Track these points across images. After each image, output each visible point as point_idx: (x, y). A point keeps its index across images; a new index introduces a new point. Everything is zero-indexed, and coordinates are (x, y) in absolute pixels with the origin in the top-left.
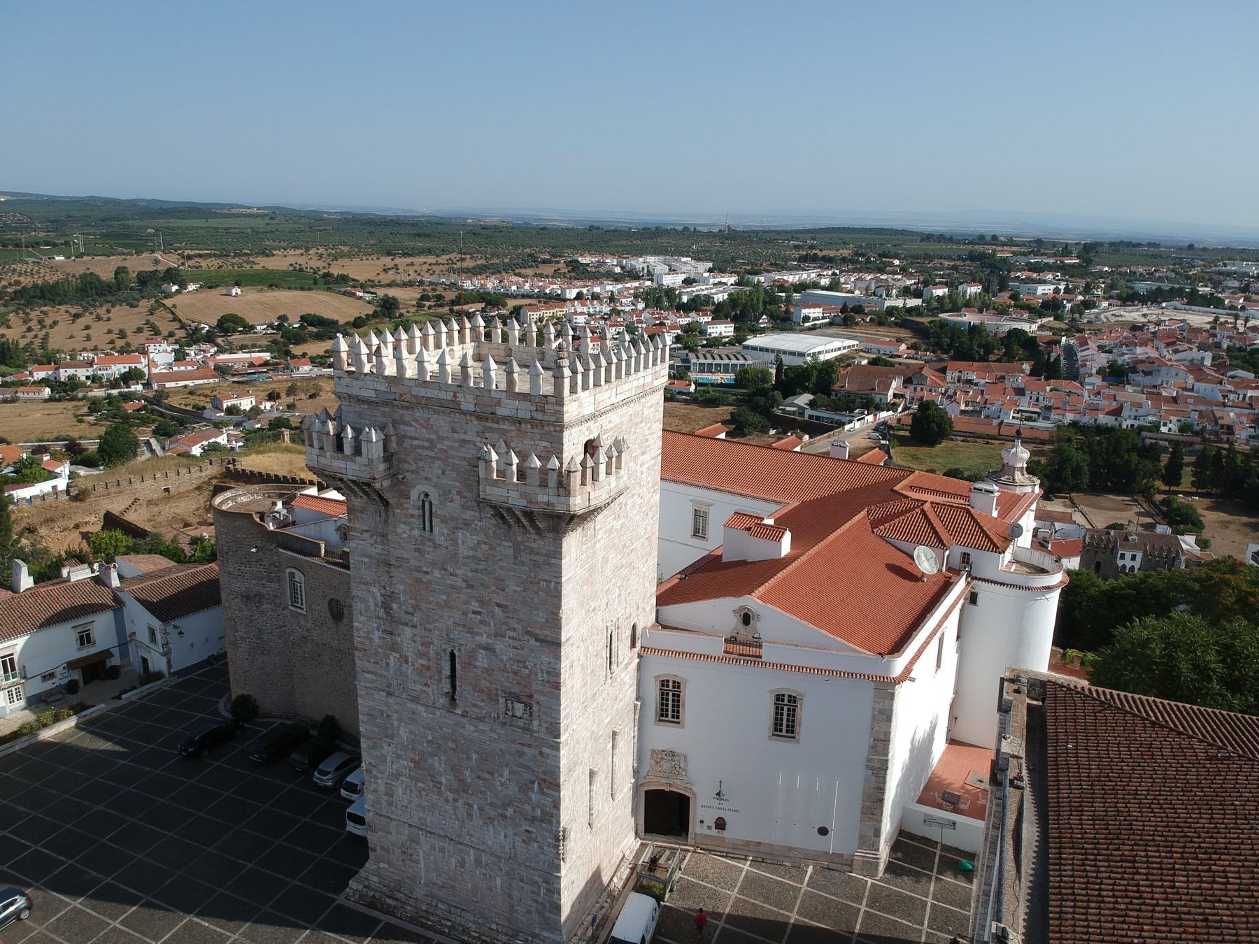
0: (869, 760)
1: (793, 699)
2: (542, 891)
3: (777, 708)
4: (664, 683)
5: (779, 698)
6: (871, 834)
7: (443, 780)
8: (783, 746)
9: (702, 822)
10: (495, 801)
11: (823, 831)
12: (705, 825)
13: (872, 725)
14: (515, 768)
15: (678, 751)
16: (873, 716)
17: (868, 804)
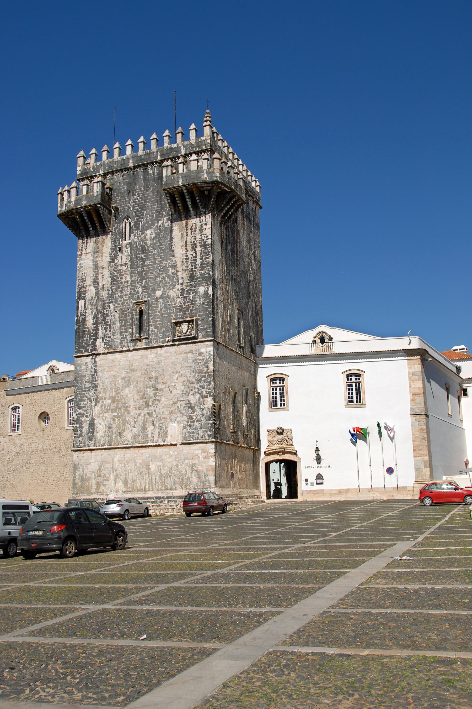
0: (411, 410)
1: (358, 376)
2: (201, 459)
3: (348, 385)
4: (273, 380)
5: (349, 376)
6: (422, 466)
7: (131, 403)
8: (356, 411)
9: (306, 480)
10: (167, 403)
11: (390, 471)
12: (309, 482)
13: (410, 384)
14: (182, 372)
15: (285, 428)
16: (410, 378)
17: (416, 443)
